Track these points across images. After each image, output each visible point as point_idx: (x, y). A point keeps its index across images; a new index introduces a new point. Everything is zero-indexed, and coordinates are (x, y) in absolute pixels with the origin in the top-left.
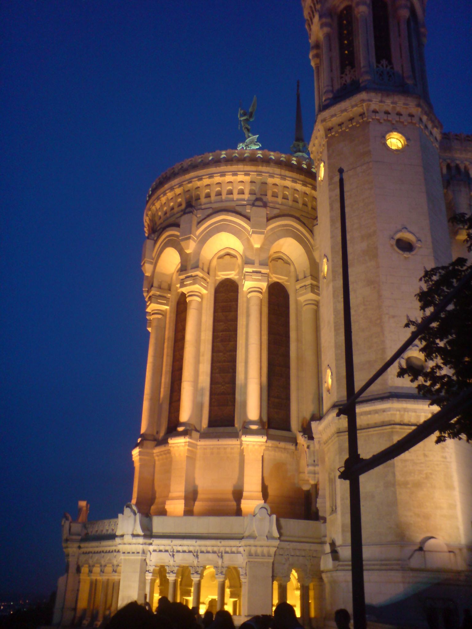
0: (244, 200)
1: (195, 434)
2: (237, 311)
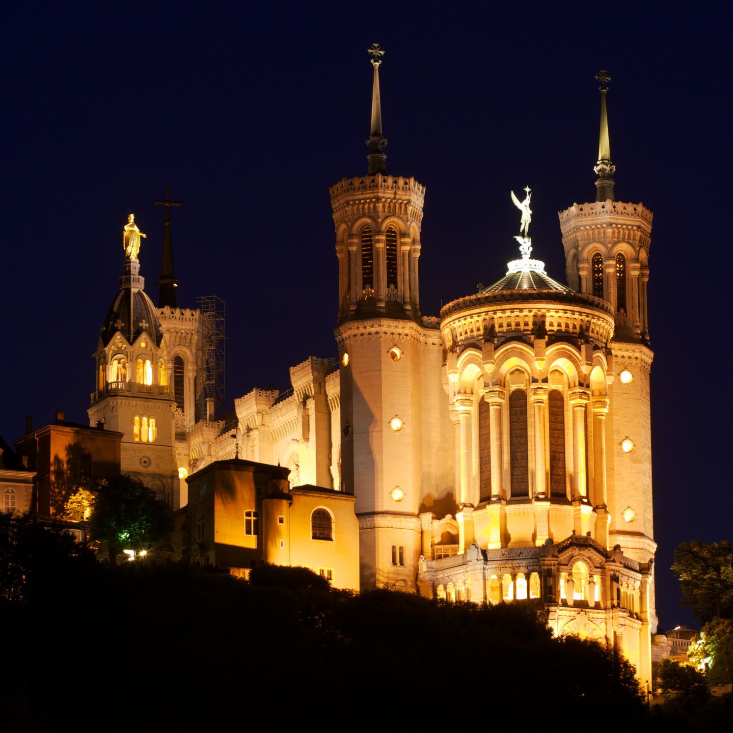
0: (528, 330)
1: (502, 501)
2: (527, 414)
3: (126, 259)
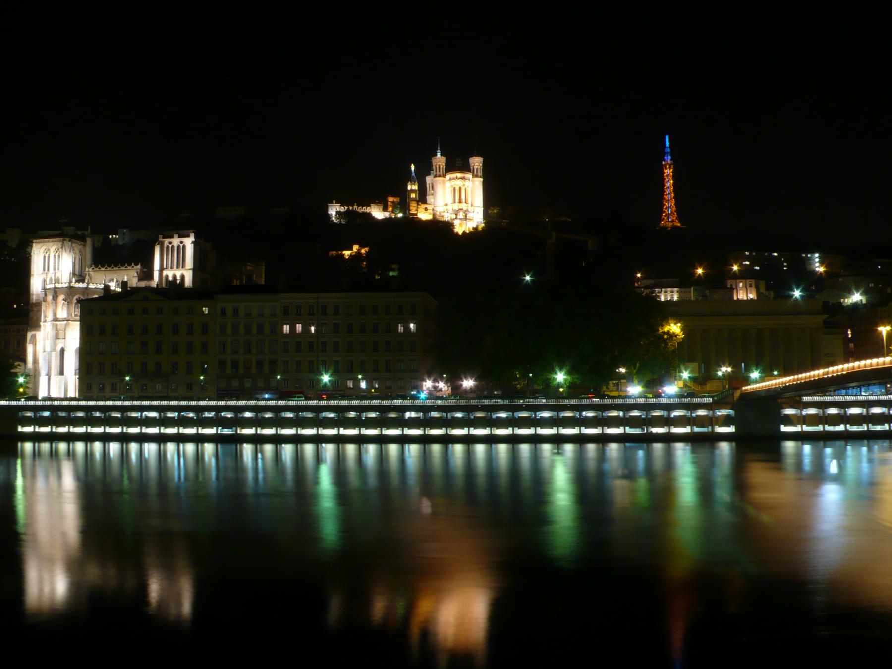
3: (411, 171)
